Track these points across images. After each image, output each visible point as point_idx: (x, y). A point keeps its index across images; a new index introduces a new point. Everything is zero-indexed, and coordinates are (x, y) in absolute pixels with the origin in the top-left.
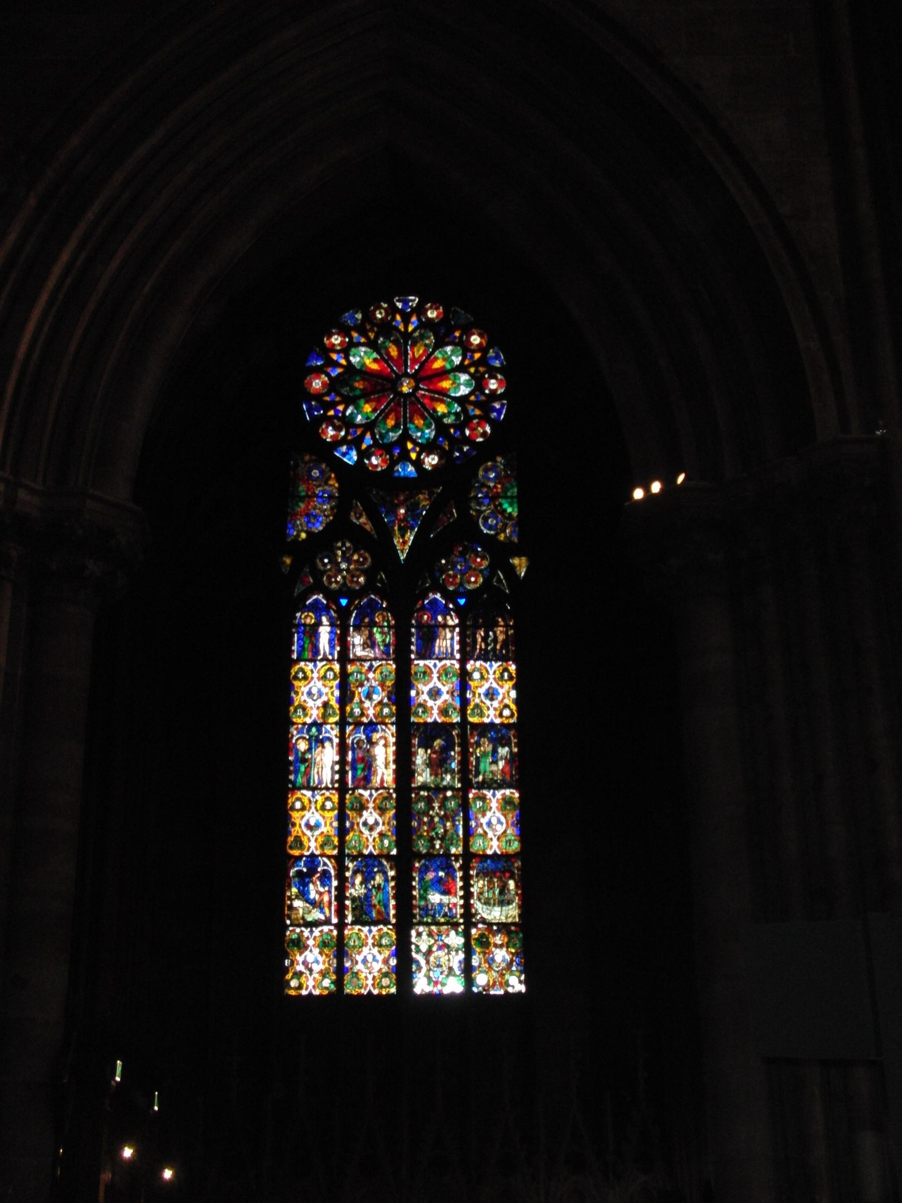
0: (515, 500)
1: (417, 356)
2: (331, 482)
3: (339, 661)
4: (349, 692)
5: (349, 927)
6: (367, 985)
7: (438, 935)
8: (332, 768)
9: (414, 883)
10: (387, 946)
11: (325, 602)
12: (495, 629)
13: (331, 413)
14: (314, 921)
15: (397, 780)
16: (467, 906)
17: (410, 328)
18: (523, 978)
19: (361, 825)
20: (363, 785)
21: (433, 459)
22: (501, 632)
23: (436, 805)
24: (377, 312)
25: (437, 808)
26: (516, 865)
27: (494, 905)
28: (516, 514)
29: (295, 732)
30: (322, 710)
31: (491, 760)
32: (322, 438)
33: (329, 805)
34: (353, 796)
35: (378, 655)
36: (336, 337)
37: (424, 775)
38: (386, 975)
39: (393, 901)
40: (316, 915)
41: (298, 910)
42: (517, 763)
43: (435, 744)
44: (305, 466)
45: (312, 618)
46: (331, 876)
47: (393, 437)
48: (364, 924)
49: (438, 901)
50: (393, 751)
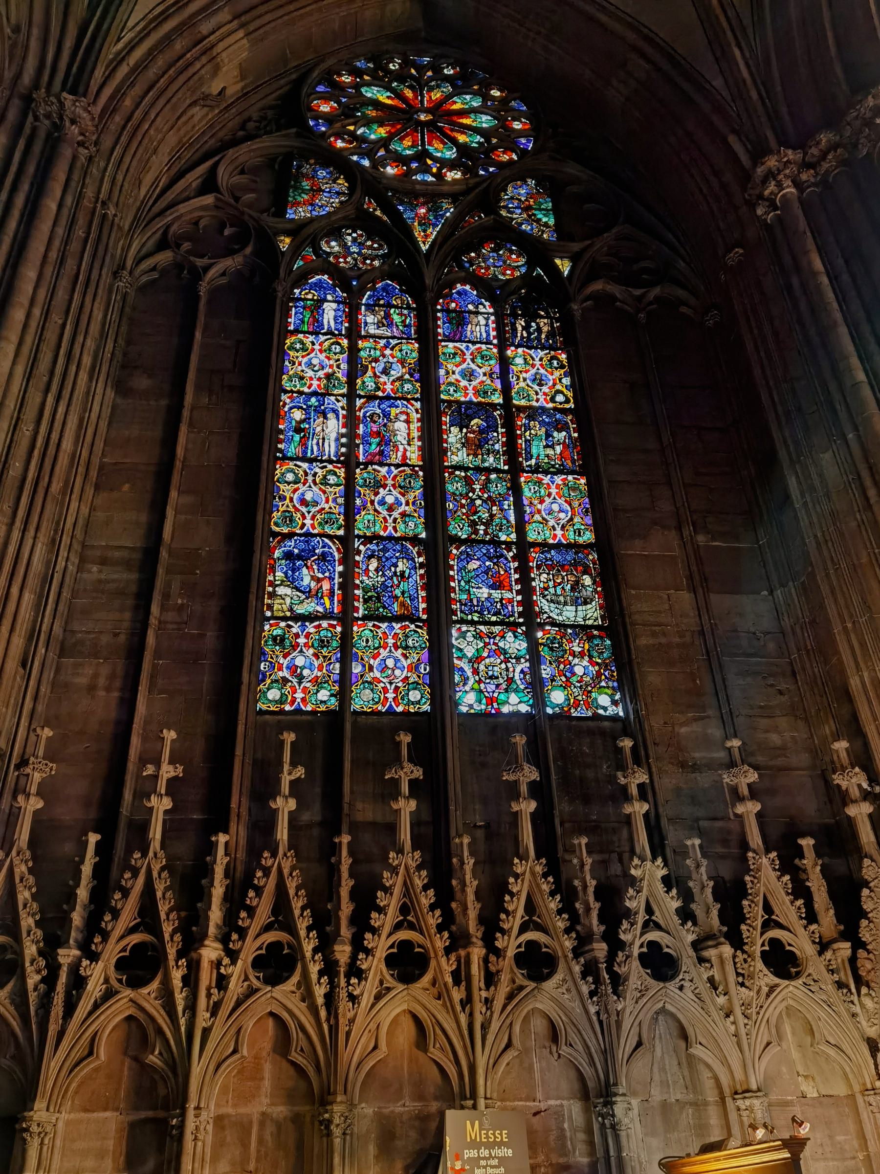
3: (348, 336)
5: (359, 622)
6: (386, 699)
7: (490, 638)
8: (337, 440)
12: (538, 320)
16: (528, 604)
19: (376, 504)
22: (545, 324)
23: (477, 487)
26: (591, 557)
27: (565, 604)
29: (288, 401)
33: (332, 479)
40: (309, 607)
41: (284, 599)
43: (472, 423)
46: (335, 561)
48: (382, 619)
49: (486, 596)
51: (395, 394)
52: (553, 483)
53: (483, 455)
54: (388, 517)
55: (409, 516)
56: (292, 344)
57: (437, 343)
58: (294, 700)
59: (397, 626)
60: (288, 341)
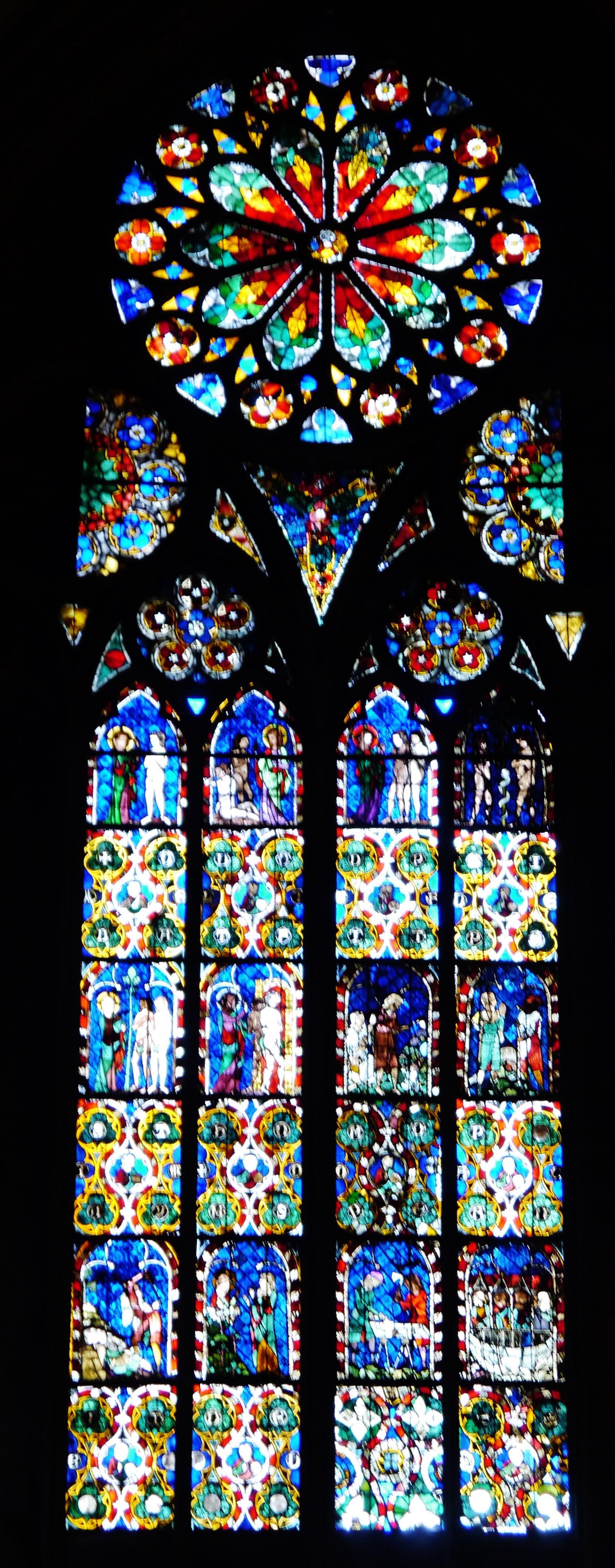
0: (559, 491)
1: (352, 183)
2: (170, 452)
3: (183, 828)
4: (205, 894)
5: (204, 1387)
6: (239, 1510)
7: (389, 1406)
8: (170, 1052)
9: (339, 1296)
10: (281, 1427)
11: (157, 705)
13: (171, 305)
14: (129, 1374)
15: (304, 1080)
17: (339, 124)
18: (566, 1499)
19: (229, 1172)
20: (235, 1089)
21: (386, 404)
22: (526, 769)
23: (387, 1132)
24: (270, 88)
25: (388, 1138)
26: (554, 1259)
27: (507, 1343)
28: (561, 521)
29: (92, 978)
30: (149, 933)
31: (502, 1040)
32: (152, 358)
33: (162, 1130)
34: (212, 1111)
35: (266, 817)
36: (180, 141)
37: (363, 1067)
38: (280, 1489)
39: (295, 1332)
42: (557, 1045)
44: (116, 418)
45: (129, 738)
46: (167, 1281)
47: (300, 358)
48: (235, 1380)
50: (298, 1019)
51: (262, 949)
52: (508, 1117)
53: (399, 1068)
54: (246, 1197)
55: (279, 1193)
56: (95, 853)
57: (334, 831)
58: (114, 1513)
59: (256, 1392)
60: (87, 849)
